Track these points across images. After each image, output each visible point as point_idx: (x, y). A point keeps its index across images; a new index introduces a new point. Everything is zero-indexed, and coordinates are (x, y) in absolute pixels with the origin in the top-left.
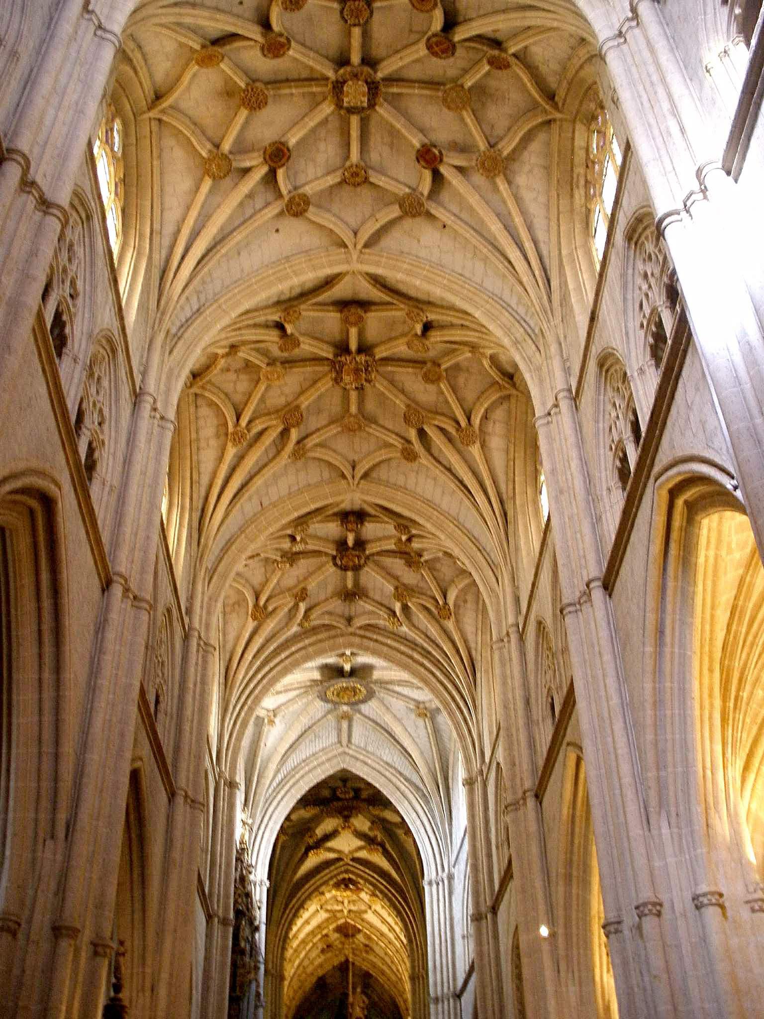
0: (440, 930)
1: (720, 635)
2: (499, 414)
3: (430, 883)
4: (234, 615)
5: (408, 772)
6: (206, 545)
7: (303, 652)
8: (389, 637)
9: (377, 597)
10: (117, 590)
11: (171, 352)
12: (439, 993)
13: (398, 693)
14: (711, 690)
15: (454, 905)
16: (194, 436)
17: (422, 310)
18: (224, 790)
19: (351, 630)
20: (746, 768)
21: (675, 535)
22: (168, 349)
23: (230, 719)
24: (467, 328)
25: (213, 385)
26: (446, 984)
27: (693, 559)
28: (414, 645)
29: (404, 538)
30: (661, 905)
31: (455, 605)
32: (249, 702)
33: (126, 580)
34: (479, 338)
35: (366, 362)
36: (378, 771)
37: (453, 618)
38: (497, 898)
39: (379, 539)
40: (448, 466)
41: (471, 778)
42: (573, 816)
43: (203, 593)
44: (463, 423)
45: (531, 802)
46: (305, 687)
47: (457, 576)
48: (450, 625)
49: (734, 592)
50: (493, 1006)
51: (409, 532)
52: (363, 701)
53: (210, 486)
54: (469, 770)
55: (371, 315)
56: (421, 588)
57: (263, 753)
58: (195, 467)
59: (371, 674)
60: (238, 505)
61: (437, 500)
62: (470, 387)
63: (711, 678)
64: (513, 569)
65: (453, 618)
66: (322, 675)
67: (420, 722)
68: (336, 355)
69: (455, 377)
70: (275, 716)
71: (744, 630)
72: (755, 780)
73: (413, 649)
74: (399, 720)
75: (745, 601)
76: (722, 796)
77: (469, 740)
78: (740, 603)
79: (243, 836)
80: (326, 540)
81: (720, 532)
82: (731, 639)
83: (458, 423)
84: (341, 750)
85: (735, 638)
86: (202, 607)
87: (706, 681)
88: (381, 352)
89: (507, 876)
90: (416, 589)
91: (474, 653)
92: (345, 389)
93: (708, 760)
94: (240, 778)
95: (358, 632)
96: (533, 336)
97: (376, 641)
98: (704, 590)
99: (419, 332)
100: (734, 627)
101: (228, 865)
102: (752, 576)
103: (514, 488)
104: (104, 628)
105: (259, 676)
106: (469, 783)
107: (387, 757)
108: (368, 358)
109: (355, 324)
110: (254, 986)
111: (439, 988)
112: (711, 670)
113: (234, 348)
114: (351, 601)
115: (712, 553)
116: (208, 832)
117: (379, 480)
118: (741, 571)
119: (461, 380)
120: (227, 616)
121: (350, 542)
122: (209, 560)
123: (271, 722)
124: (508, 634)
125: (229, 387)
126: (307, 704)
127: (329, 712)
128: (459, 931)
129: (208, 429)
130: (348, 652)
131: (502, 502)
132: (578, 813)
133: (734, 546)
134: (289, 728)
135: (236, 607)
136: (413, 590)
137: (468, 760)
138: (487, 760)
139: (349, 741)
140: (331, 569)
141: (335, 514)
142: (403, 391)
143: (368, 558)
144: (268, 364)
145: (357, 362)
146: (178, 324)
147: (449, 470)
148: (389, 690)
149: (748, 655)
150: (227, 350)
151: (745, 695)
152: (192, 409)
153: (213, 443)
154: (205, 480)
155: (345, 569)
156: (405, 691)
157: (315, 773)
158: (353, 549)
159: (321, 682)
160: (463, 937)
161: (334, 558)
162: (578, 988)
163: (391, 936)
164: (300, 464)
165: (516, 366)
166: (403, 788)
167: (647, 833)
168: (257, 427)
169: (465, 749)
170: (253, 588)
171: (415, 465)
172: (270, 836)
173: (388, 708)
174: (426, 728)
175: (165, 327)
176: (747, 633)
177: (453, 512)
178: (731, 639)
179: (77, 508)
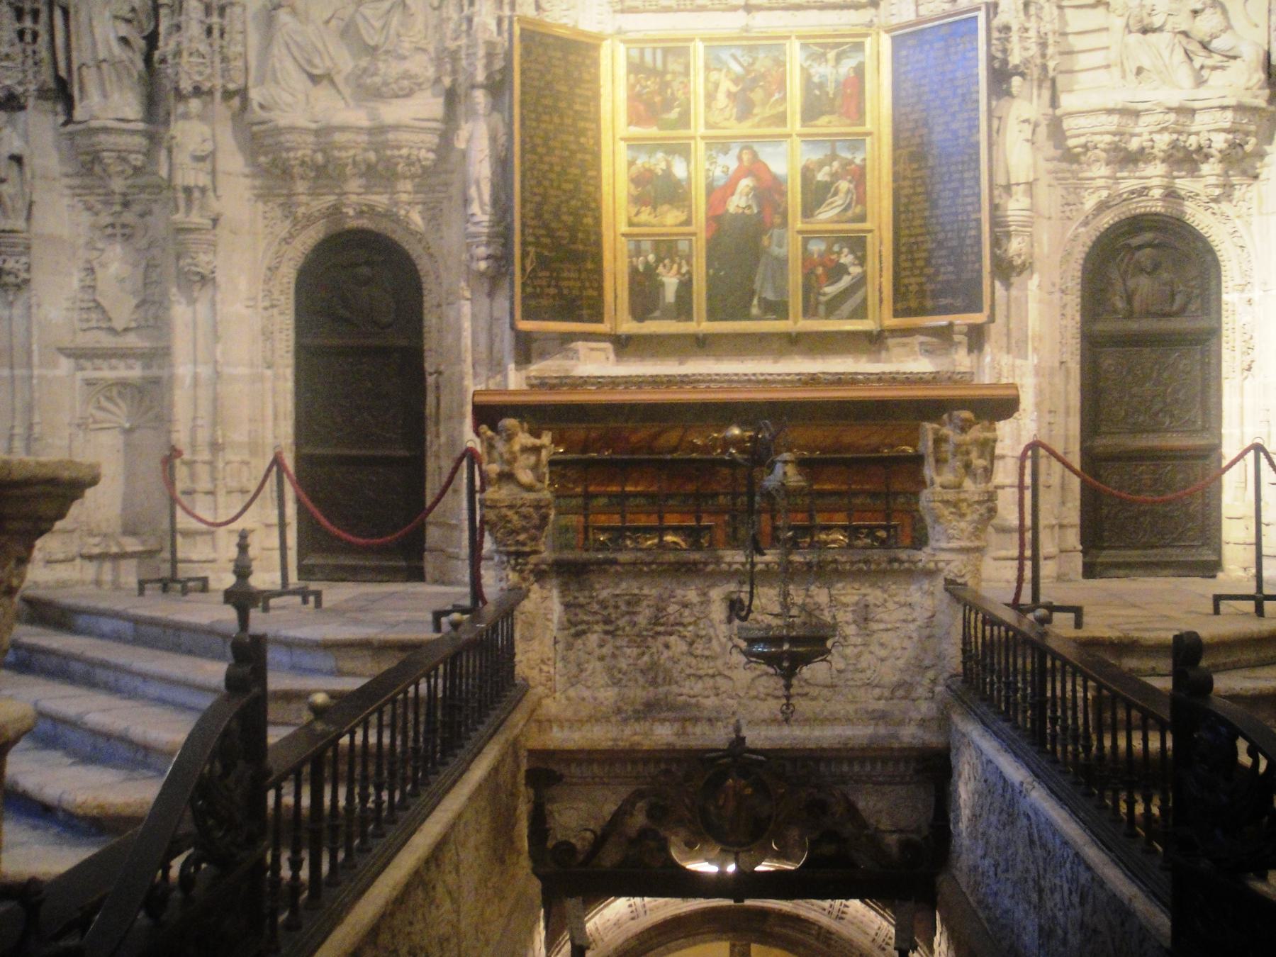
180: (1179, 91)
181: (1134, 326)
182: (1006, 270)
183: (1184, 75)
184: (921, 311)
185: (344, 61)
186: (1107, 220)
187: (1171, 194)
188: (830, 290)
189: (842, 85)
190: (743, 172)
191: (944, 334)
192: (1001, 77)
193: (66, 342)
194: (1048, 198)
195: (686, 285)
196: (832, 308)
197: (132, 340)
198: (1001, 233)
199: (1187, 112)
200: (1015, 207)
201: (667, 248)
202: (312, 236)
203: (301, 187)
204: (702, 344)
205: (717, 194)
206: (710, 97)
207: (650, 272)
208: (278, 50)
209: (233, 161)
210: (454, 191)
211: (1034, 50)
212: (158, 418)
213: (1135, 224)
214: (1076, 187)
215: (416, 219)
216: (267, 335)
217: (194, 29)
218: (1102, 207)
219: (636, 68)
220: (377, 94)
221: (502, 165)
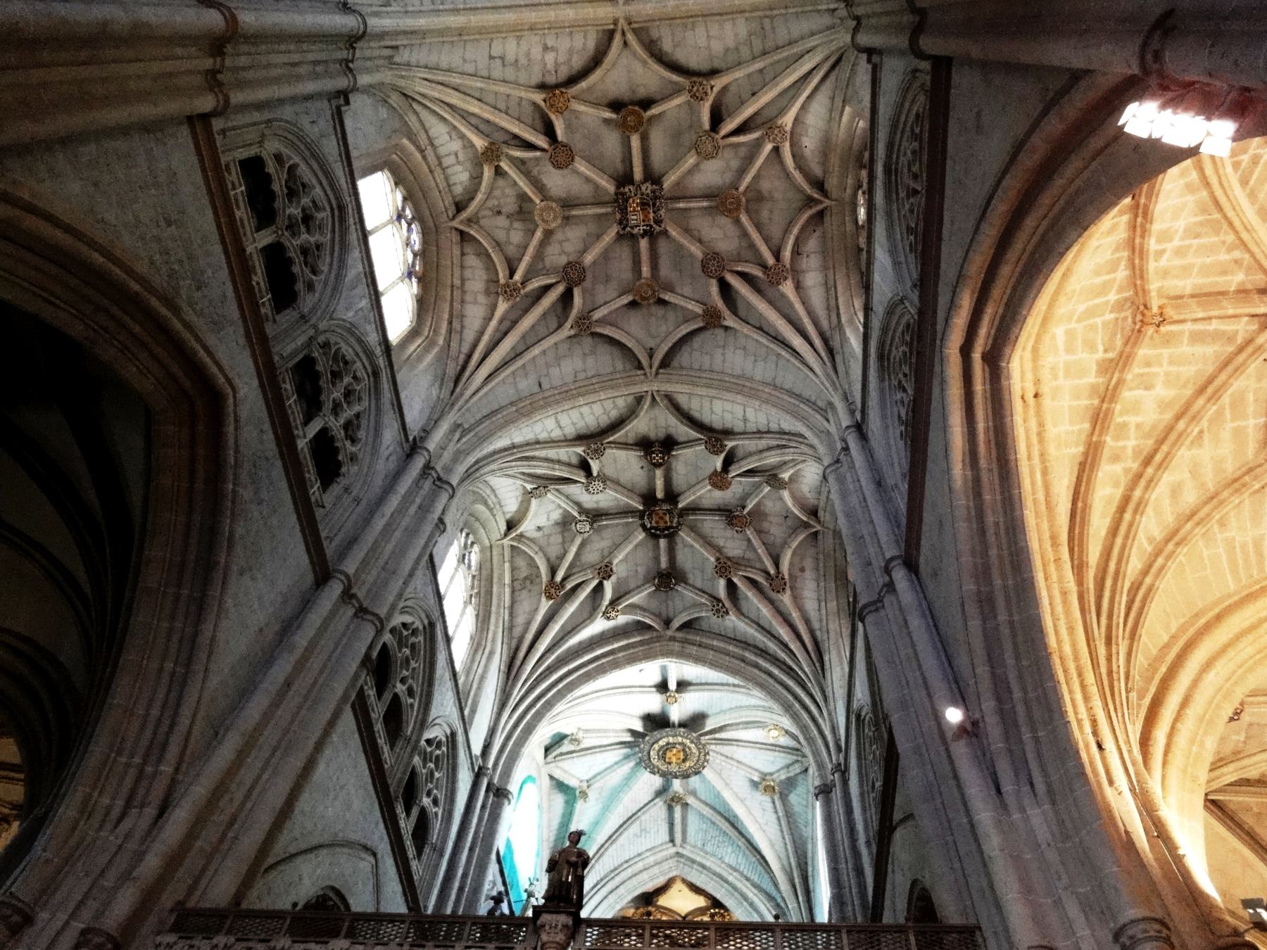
2: (812, 244)
8: (713, 639)
9: (699, 584)
16: (457, 282)
18: (486, 797)
19: (669, 633)
23: (510, 717)
28: (746, 644)
31: (790, 575)
35: (653, 192)
37: (788, 592)
42: (977, 481)
44: (771, 261)
45: (900, 575)
47: (790, 536)
48: (786, 599)
53: (474, 346)
56: (749, 560)
58: (456, 317)
62: (774, 215)
65: (788, 592)
66: (645, 726)
67: (766, 799)
68: (618, 187)
69: (757, 212)
70: (588, 787)
73: (744, 649)
74: (742, 801)
77: (820, 741)
84: (673, 850)
88: (668, 182)
90: (740, 562)
91: (818, 634)
92: (632, 236)
95: (679, 635)
109: (635, 129)
117: (682, 368)
119: (765, 214)
120: (517, 593)
121: (660, 494)
123: (584, 794)
124: (846, 449)
125: (501, 235)
129: (476, 281)
130: (672, 685)
131: (826, 341)
132: (985, 477)
135: (528, 582)
142: (700, 241)
145: (642, 194)
152: (457, 252)
153: (482, 299)
154: (469, 336)
157: (639, 877)
158: (663, 501)
161: (641, 515)
166: (750, 895)
168: (535, 284)
170: (548, 560)
174: (776, 812)
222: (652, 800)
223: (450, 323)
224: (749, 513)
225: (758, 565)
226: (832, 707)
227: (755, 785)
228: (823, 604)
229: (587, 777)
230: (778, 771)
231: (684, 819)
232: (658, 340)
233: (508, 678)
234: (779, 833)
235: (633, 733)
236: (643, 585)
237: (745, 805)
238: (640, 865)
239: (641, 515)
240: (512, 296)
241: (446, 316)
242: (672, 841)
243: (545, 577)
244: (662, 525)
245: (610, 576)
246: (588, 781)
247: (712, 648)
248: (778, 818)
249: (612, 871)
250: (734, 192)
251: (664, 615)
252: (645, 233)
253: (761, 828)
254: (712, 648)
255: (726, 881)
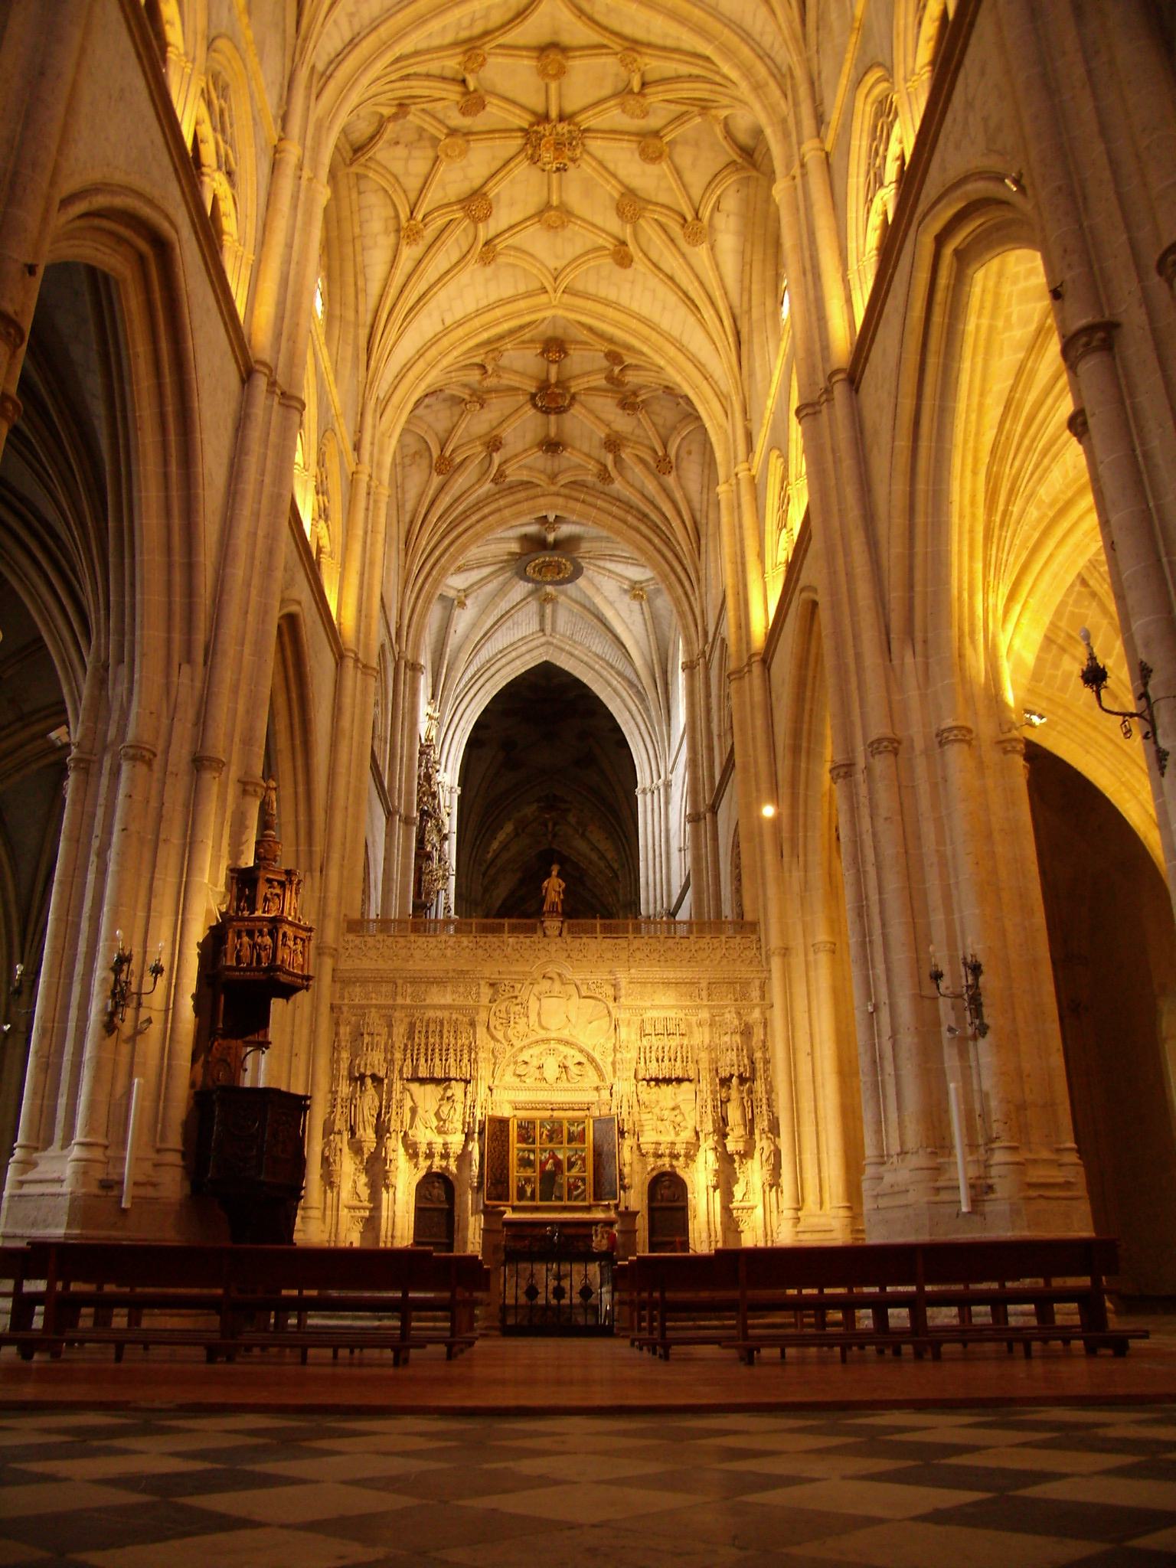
0: (654, 845)
1: (989, 436)
3: (644, 791)
4: (414, 469)
5: (620, 665)
6: (377, 368)
7: (497, 516)
9: (586, 449)
10: (261, 383)
11: (318, 97)
12: (651, 912)
13: (610, 571)
14: (973, 497)
15: (671, 815)
17: (639, 53)
18: (405, 673)
19: (554, 489)
20: (1011, 597)
21: (940, 296)
22: (314, 91)
24: (697, 78)
25: (378, 163)
26: (659, 903)
27: (961, 327)
28: (629, 507)
29: (617, 369)
30: (899, 742)
32: (434, 573)
33: (271, 371)
34: (712, 91)
35: (570, 132)
36: (586, 663)
37: (673, 473)
38: (717, 795)
39: (588, 373)
40: (670, 273)
41: (692, 661)
43: (374, 427)
44: (689, 218)
46: (501, 562)
47: (680, 421)
49: (1011, 382)
50: (709, 912)
51: (621, 362)
52: (571, 579)
54: (689, 651)
55: (576, 63)
56: (639, 436)
57: (453, 641)
58: (360, 272)
59: (577, 548)
60: (414, 324)
61: (656, 317)
63: (974, 482)
64: (744, 397)
66: (522, 547)
70: (466, 596)
71: (1019, 429)
72: (1021, 614)
74: (611, 604)
75: (1023, 392)
76: (980, 624)
77: (690, 618)
78: (1017, 395)
79: (429, 730)
80: (522, 374)
81: (997, 295)
82: (1003, 438)
83: (685, 219)
84: (543, 640)
85: (1007, 438)
86: (372, 444)
87: (968, 486)
89: (729, 766)
90: (629, 436)
93: (966, 578)
94: (425, 660)
96: (778, 76)
97: (583, 502)
98: (973, 370)
99: (636, 89)
100: (1007, 426)
101: (411, 758)
102: (1035, 361)
103: (750, 300)
104: (245, 424)
105: (446, 542)
106: (689, 667)
107: (597, 648)
108: (572, 127)
110: (442, 894)
111: (651, 906)
112: (975, 473)
113: (402, 107)
114: (554, 452)
115: (985, 322)
116: (386, 720)
118: (1021, 355)
121: (553, 380)
122: (382, 387)
123: (462, 605)
126: (504, 584)
127: (530, 594)
128: (675, 845)
130: (551, 518)
133: (1014, 319)
134: (483, 611)
136: (628, 440)
137: (688, 642)
138: (710, 639)
139: (553, 629)
140: (530, 412)
141: (532, 341)
143: (573, 397)
144: (448, 135)
145: (557, 134)
146: (325, 59)
147: (671, 278)
148: (599, 567)
149: (1023, 462)
150: (393, 110)
151: (1015, 510)
152: (354, 196)
154: (375, 288)
155: (546, 411)
156: (619, 568)
157: (512, 665)
159: (520, 555)
160: (680, 851)
162: (802, 873)
163: (602, 864)
164: (489, 270)
165: (758, 133)
167: (888, 663)
169: (685, 627)
170: (437, 434)
171: (629, 272)
172: (461, 738)
173: (598, 589)
174: (643, 613)
175: (310, 58)
176: (1022, 437)
177: (676, 333)
178: (1003, 438)
179: (203, 267)
180: (671, 1138)
181: (664, 1204)
182: (624, 1188)
183: (672, 1132)
184: (601, 1200)
185: (434, 1123)
186: (654, 1173)
187: (671, 1166)
188: (575, 1193)
189: (579, 1133)
190: (550, 1158)
191: (608, 1207)
192: (622, 1133)
193: (346, 1203)
194: (637, 1167)
195: (533, 1192)
196: (576, 1198)
197: (366, 1204)
198: (622, 1177)
199: (673, 1143)
200: (626, 1170)
201: (528, 1180)
202: (423, 1173)
203: (421, 1159)
204: (537, 1209)
205: (543, 1164)
206: (541, 1135)
207: (523, 1186)
208: (417, 1119)
209: (401, 1150)
210: (467, 1161)
211: (631, 1126)
212: (373, 1228)
213: (663, 1174)
214: (645, 1164)
215: (453, 1168)
216: (408, 1203)
217: (394, 1113)
218: (653, 1169)
219: (520, 1127)
220: (445, 1133)
221: (482, 1155)
222: (524, 599)
223: (356, 284)
224: (642, 401)
225: (646, 442)
226: (703, 590)
227: (626, 591)
228: (705, 490)
229: (462, 587)
230: (647, 580)
231: (554, 611)
232: (564, 262)
233: (406, 554)
234: (643, 632)
235: (511, 554)
236: (530, 448)
237: (616, 610)
238: (514, 654)
239: (533, 396)
240: (415, 240)
241: (351, 280)
242: (542, 630)
243: (436, 453)
244: (553, 405)
245: (498, 449)
246: (464, 590)
247: (594, 506)
248: (644, 619)
249: (488, 662)
250: (656, 142)
251: (549, 471)
252: (558, 169)
253: (628, 627)
254: (594, 506)
255: (593, 669)
